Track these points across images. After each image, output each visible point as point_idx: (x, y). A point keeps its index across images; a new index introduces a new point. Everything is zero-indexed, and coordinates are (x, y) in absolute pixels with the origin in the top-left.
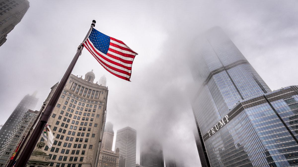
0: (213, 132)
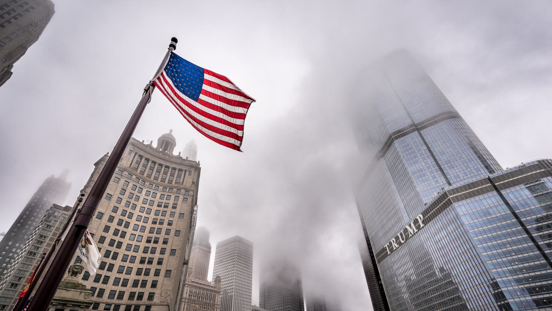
0: (395, 245)
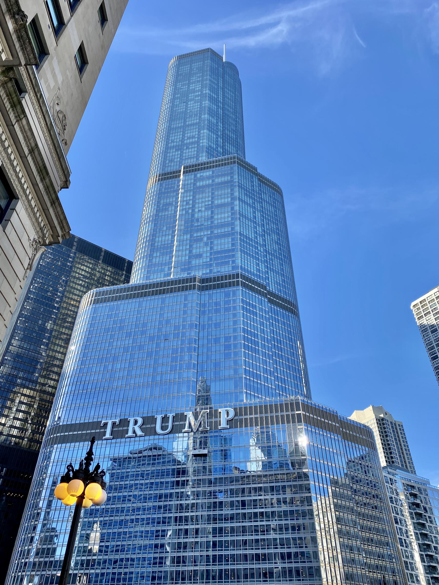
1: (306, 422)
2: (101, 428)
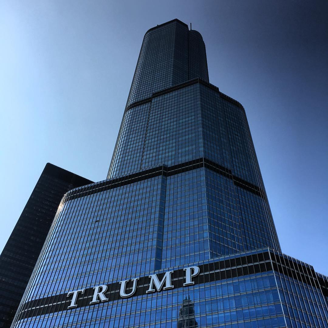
0: (99, 295)
1: (225, 168)
2: (67, 299)
